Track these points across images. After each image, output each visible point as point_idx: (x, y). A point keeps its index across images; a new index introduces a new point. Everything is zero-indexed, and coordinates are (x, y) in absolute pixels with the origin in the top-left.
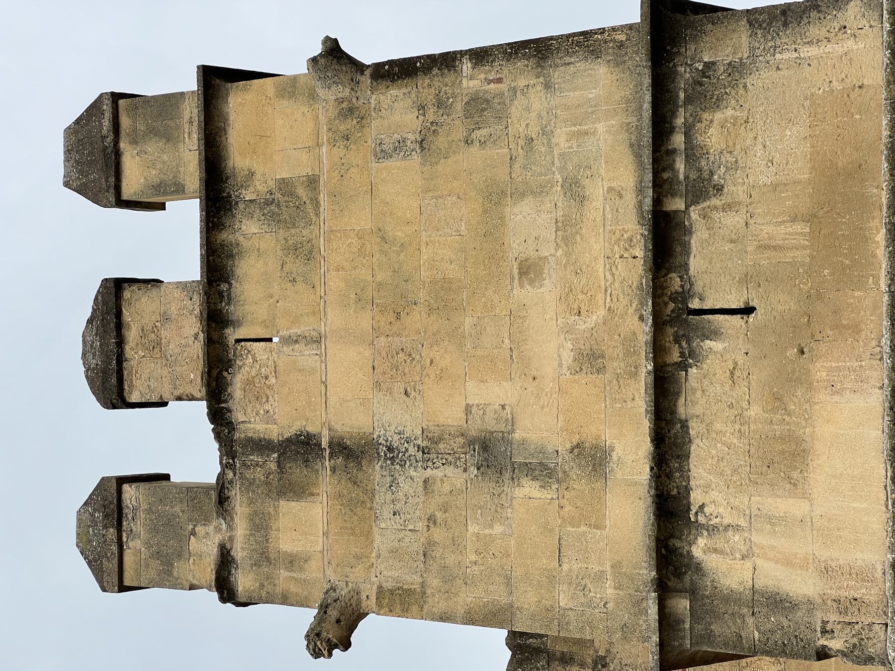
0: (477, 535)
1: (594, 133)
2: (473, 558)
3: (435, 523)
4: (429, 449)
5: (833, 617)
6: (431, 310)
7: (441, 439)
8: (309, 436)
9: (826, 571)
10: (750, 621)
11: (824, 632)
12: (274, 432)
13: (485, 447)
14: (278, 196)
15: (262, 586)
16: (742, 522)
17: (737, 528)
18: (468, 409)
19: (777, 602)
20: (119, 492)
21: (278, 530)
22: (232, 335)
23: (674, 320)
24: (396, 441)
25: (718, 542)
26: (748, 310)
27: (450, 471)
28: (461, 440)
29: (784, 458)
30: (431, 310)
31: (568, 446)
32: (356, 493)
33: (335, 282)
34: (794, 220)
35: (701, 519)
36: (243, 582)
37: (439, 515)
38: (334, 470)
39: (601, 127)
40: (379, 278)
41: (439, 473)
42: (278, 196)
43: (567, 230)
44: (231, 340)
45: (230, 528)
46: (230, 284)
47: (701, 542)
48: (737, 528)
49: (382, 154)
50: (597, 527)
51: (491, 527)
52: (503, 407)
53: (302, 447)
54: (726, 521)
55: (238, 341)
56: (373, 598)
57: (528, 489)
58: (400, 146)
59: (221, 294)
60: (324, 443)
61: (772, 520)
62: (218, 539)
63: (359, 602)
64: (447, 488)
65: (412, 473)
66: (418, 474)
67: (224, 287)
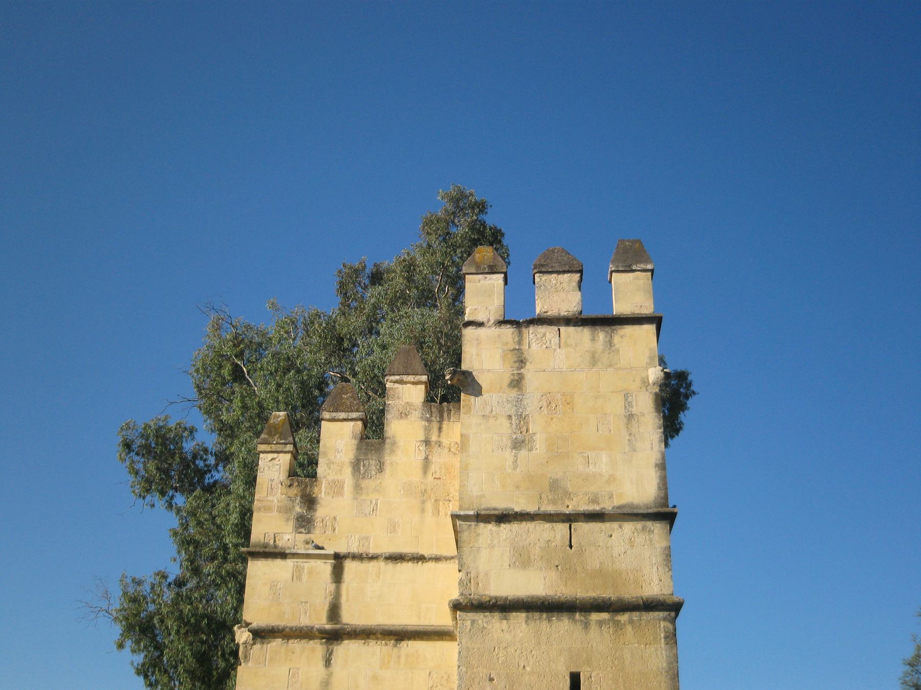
12: (525, 347)
23: (569, 518)
26: (571, 547)
29: (522, 559)
38: (513, 374)
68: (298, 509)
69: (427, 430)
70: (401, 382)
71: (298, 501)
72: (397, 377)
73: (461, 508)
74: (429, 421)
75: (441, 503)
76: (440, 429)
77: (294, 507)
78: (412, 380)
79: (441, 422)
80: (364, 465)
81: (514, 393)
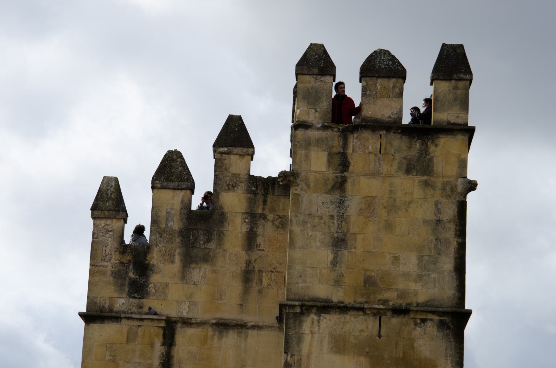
0: (316, 236)
1: (435, 287)
2: (310, 234)
3: (320, 219)
4: (343, 218)
5: (296, 358)
6: (386, 221)
7: (346, 223)
8: (348, 167)
9: (308, 357)
10: (294, 332)
11: (292, 355)
12: (350, 151)
13: (343, 240)
14: (428, 157)
15: (299, 142)
16: (321, 331)
17: (319, 329)
18: (355, 234)
19: (300, 341)
20: (330, 75)
21: (317, 151)
22: (383, 132)
24: (346, 204)
25: (316, 323)
26: (380, 336)
27: (336, 226)
28: (345, 231)
30: (386, 221)
31: (343, 272)
32: (330, 187)
33: (397, 181)
34: (404, 353)
35: (322, 318)
36: (300, 133)
37: (322, 221)
38: (337, 177)
39: (436, 290)
40: (398, 200)
41: (336, 222)
42: (428, 157)
43: (406, 276)
44: (381, 133)
45: (318, 129)
46: (400, 133)
47: (316, 317)
48: (319, 329)
49: (437, 204)
50: (320, 281)
51: (319, 241)
52: (355, 248)
53: (345, 165)
54: (321, 326)
55: (381, 135)
56: (296, 192)
57: (331, 256)
58: (438, 211)
59: (397, 130)
60: (346, 173)
61: (321, 341)
62: (314, 122)
63: (294, 186)
64: (331, 224)
65: (336, 211)
66: (335, 213)
67: (399, 131)
68: (131, 275)
69: (251, 202)
70: (228, 153)
71: (131, 267)
72: (225, 149)
73: (288, 300)
74: (255, 193)
75: (264, 274)
76: (265, 202)
77: (127, 273)
78: (240, 152)
79: (265, 196)
80: (193, 235)
81: (336, 196)
